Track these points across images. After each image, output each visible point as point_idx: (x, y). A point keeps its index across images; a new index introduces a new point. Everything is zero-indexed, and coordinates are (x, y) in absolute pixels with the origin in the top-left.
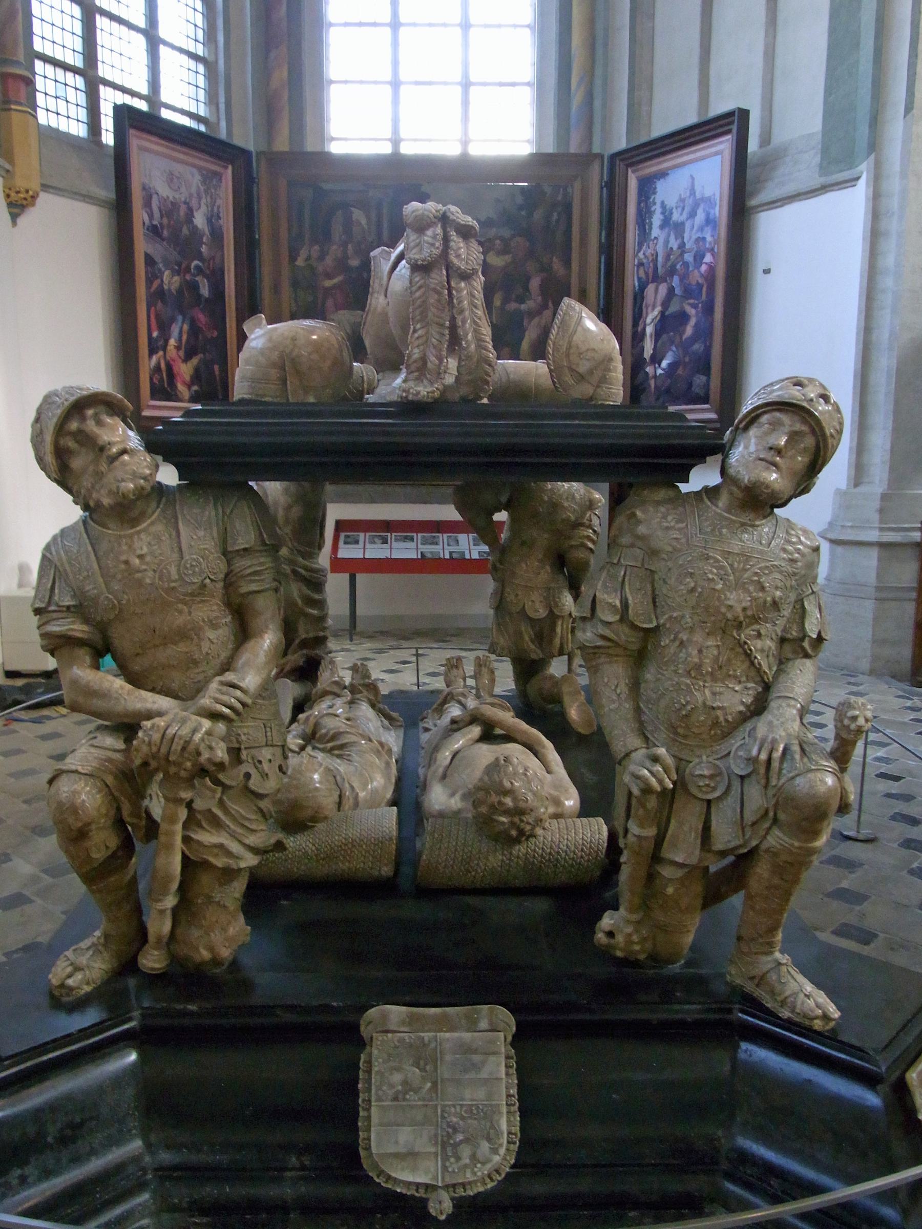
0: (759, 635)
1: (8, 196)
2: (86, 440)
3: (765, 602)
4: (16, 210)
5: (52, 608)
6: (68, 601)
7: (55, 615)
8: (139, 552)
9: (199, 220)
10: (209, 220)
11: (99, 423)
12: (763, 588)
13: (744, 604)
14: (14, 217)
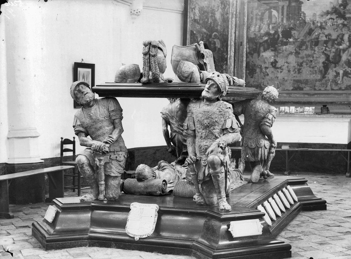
0: (214, 129)
2: (79, 91)
3: (213, 121)
5: (77, 125)
6: (79, 123)
7: (77, 127)
8: (92, 112)
9: (218, 16)
10: (222, 15)
11: (82, 88)
12: (212, 118)
13: (208, 122)
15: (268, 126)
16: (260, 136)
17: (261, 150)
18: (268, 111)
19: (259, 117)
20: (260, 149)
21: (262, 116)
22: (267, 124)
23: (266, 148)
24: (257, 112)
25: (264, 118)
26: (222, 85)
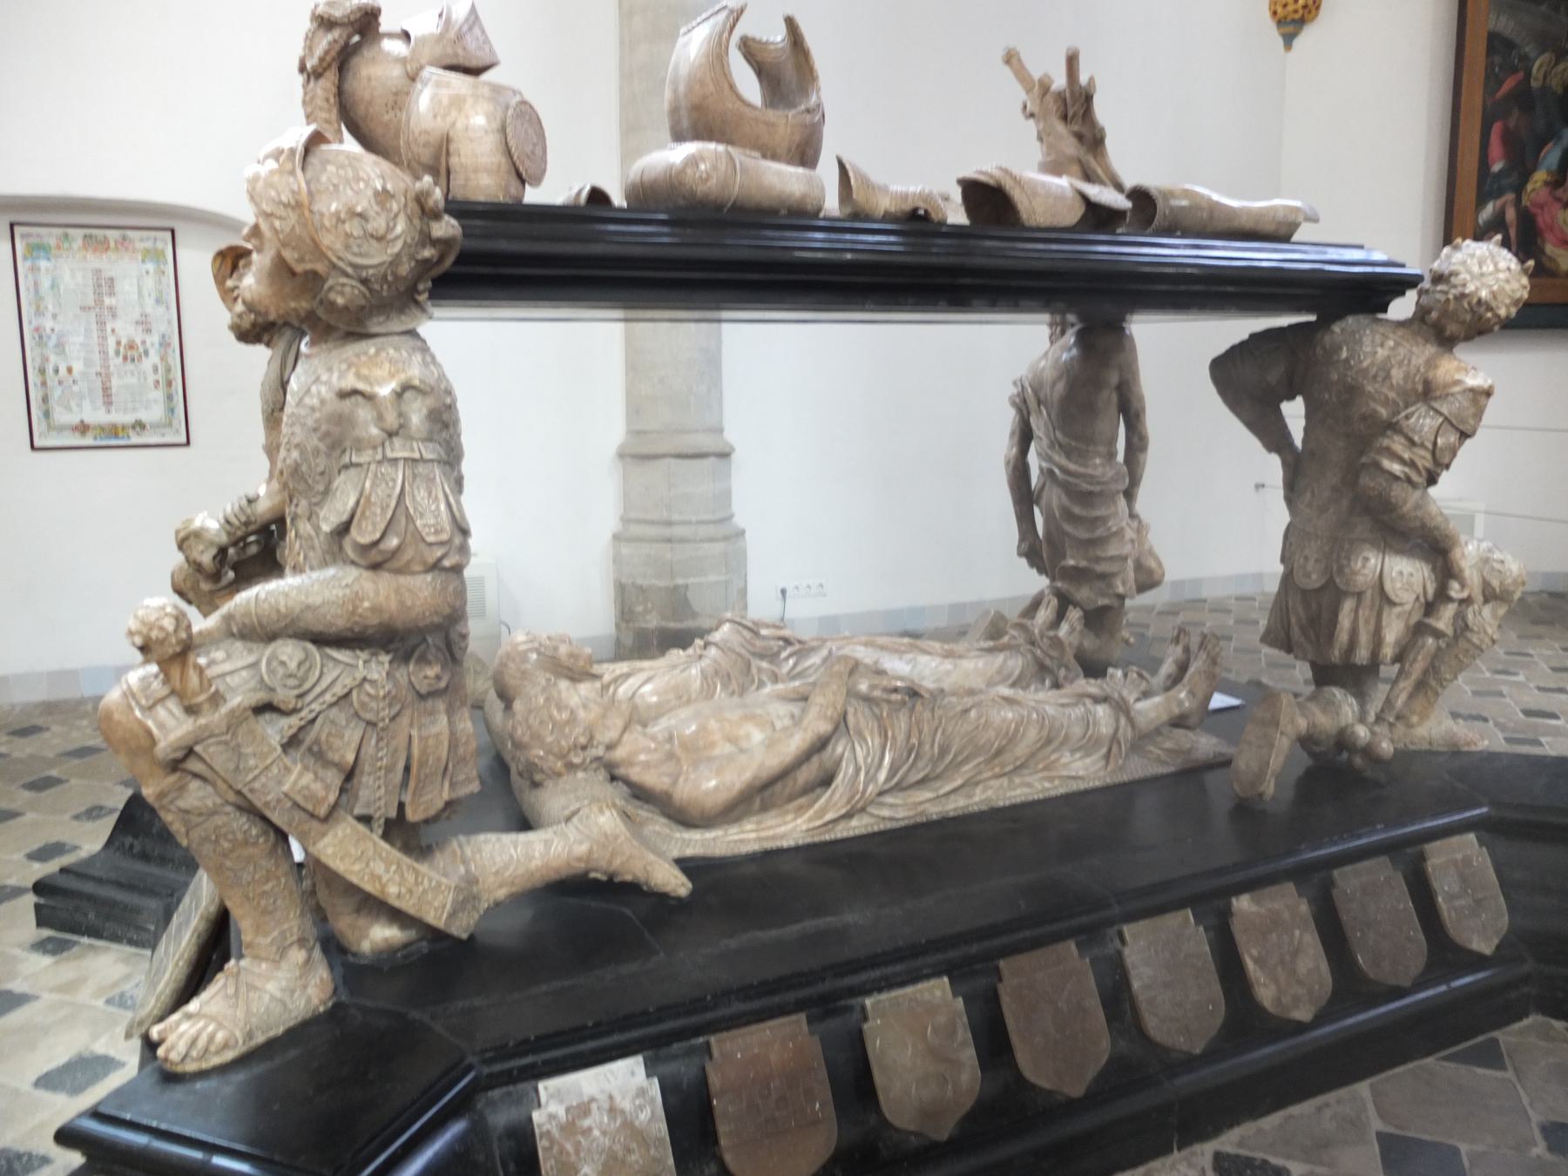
1: (1275, 13)
4: (1290, 29)
14: (1288, 39)
15: (1396, 478)
16: (1362, 526)
17: (1356, 611)
18: (1420, 388)
19: (1364, 418)
20: (1348, 605)
21: (1383, 412)
22: (1396, 468)
23: (1392, 604)
24: (1352, 391)
25: (1392, 427)
26: (277, 224)
